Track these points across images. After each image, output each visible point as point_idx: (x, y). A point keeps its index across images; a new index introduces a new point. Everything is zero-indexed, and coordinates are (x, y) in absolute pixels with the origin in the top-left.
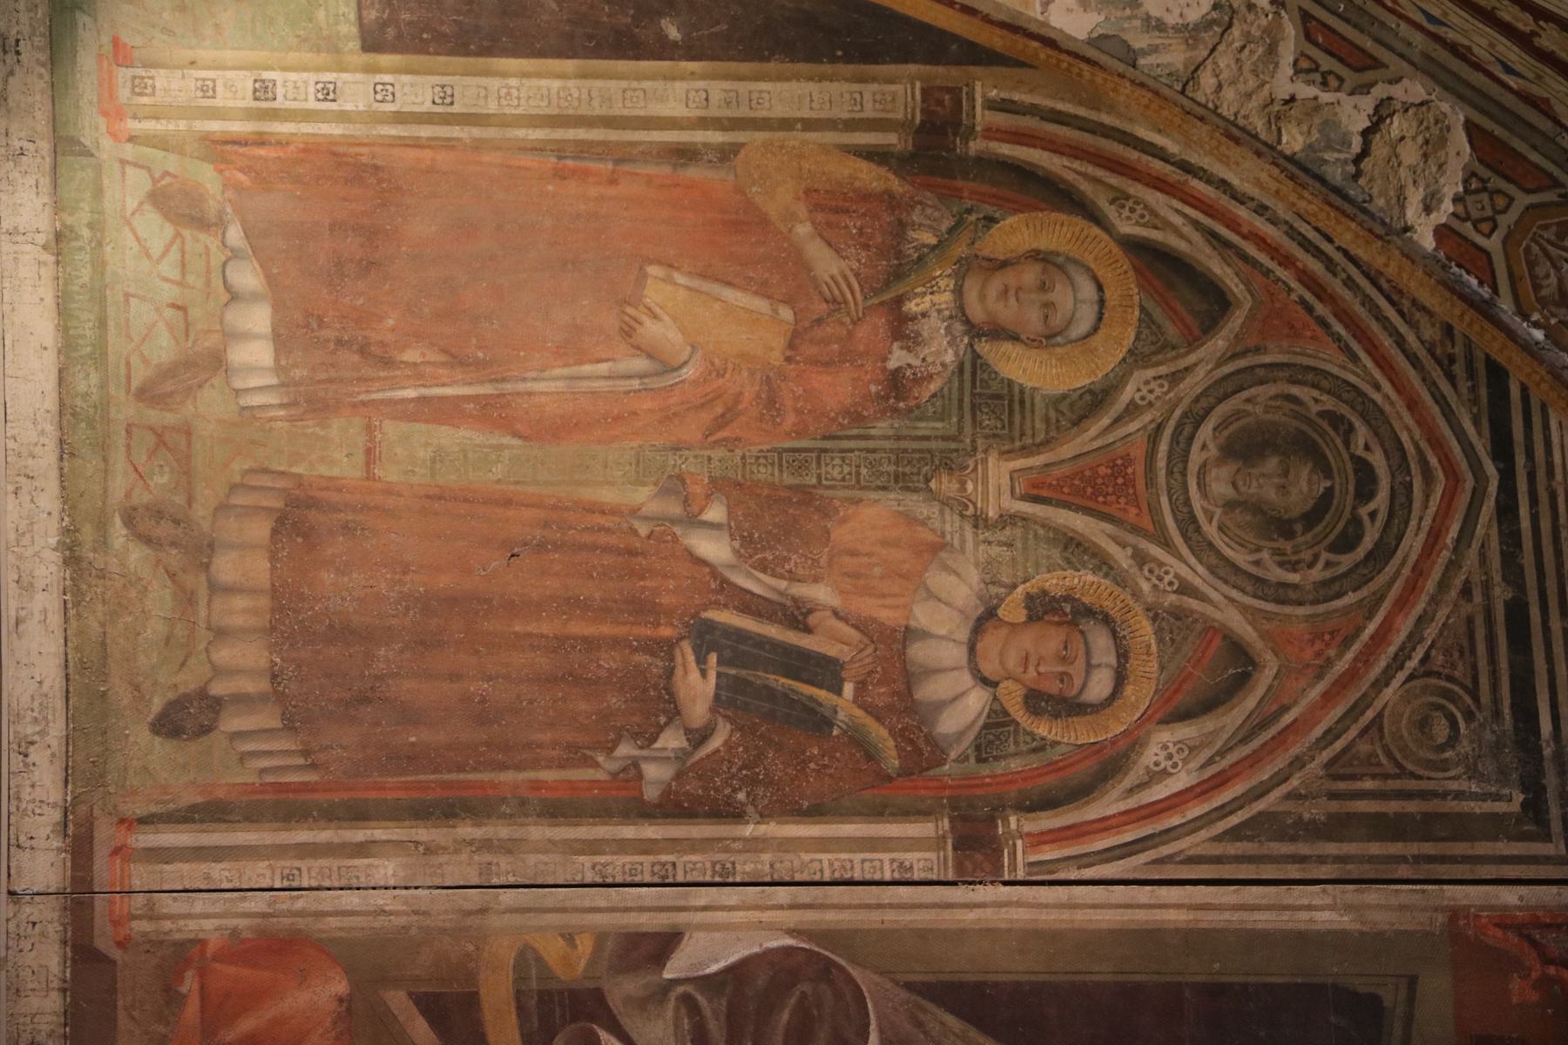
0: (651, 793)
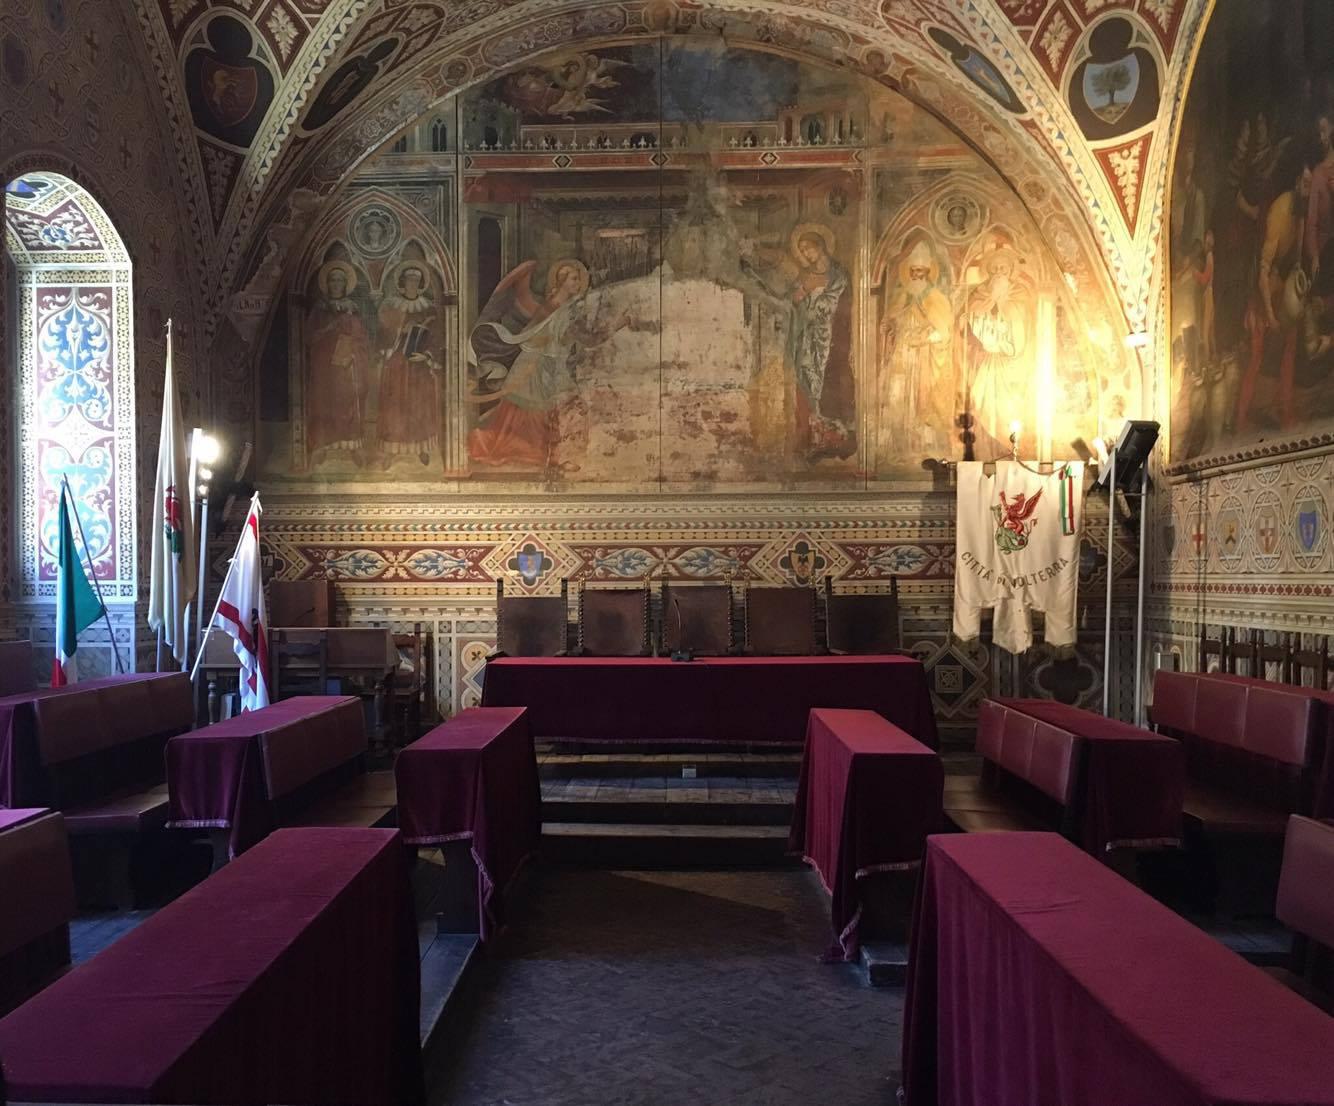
0: (440, 367)
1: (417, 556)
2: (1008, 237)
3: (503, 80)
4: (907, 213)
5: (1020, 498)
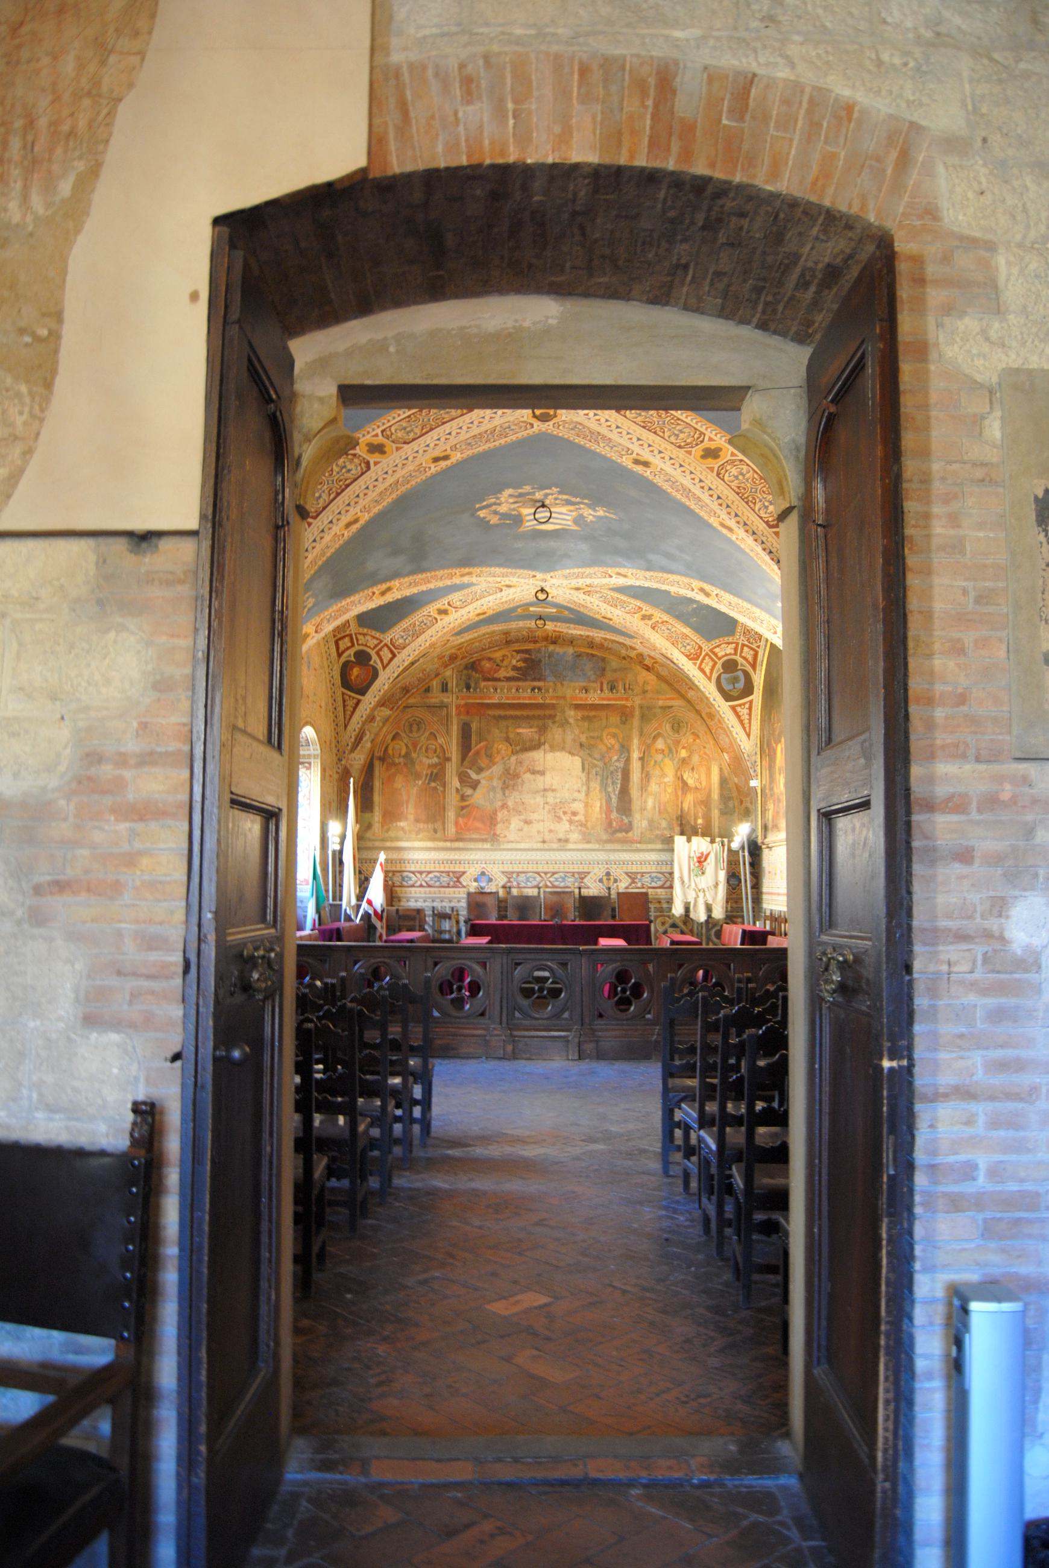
1: (431, 875)
2: (698, 736)
3: (474, 662)
4: (654, 724)
5: (702, 853)
